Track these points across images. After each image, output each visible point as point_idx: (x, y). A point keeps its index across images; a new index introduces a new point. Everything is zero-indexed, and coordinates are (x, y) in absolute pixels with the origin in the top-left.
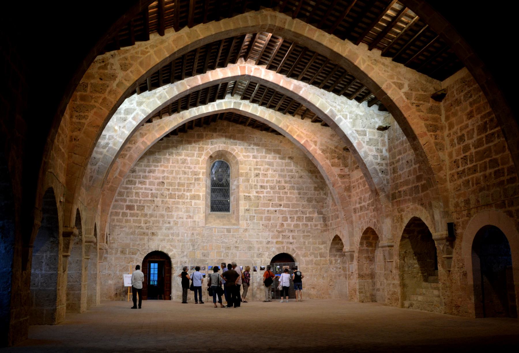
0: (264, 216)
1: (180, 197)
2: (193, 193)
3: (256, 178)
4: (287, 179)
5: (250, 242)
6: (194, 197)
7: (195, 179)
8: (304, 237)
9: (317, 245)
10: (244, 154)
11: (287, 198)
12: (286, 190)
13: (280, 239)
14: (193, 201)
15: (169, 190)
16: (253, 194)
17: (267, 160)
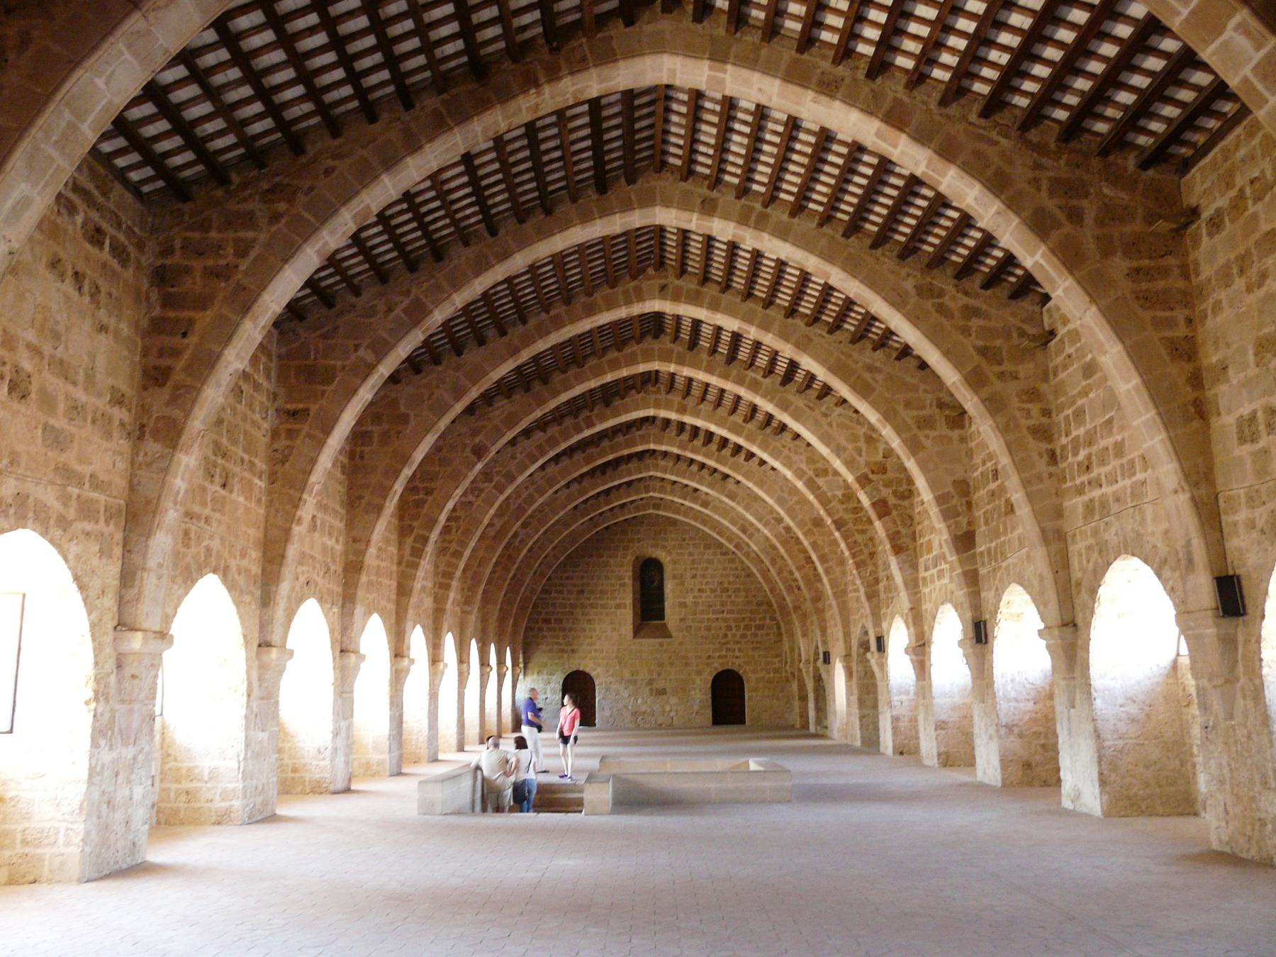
0: (703, 625)
1: (604, 607)
2: (618, 601)
3: (693, 581)
4: (731, 579)
5: (686, 658)
6: (619, 606)
7: (620, 585)
8: (754, 649)
9: (769, 659)
10: (679, 551)
11: (732, 602)
12: (730, 593)
13: (724, 653)
14: (619, 611)
15: (589, 599)
16: (689, 599)
17: (706, 557)
